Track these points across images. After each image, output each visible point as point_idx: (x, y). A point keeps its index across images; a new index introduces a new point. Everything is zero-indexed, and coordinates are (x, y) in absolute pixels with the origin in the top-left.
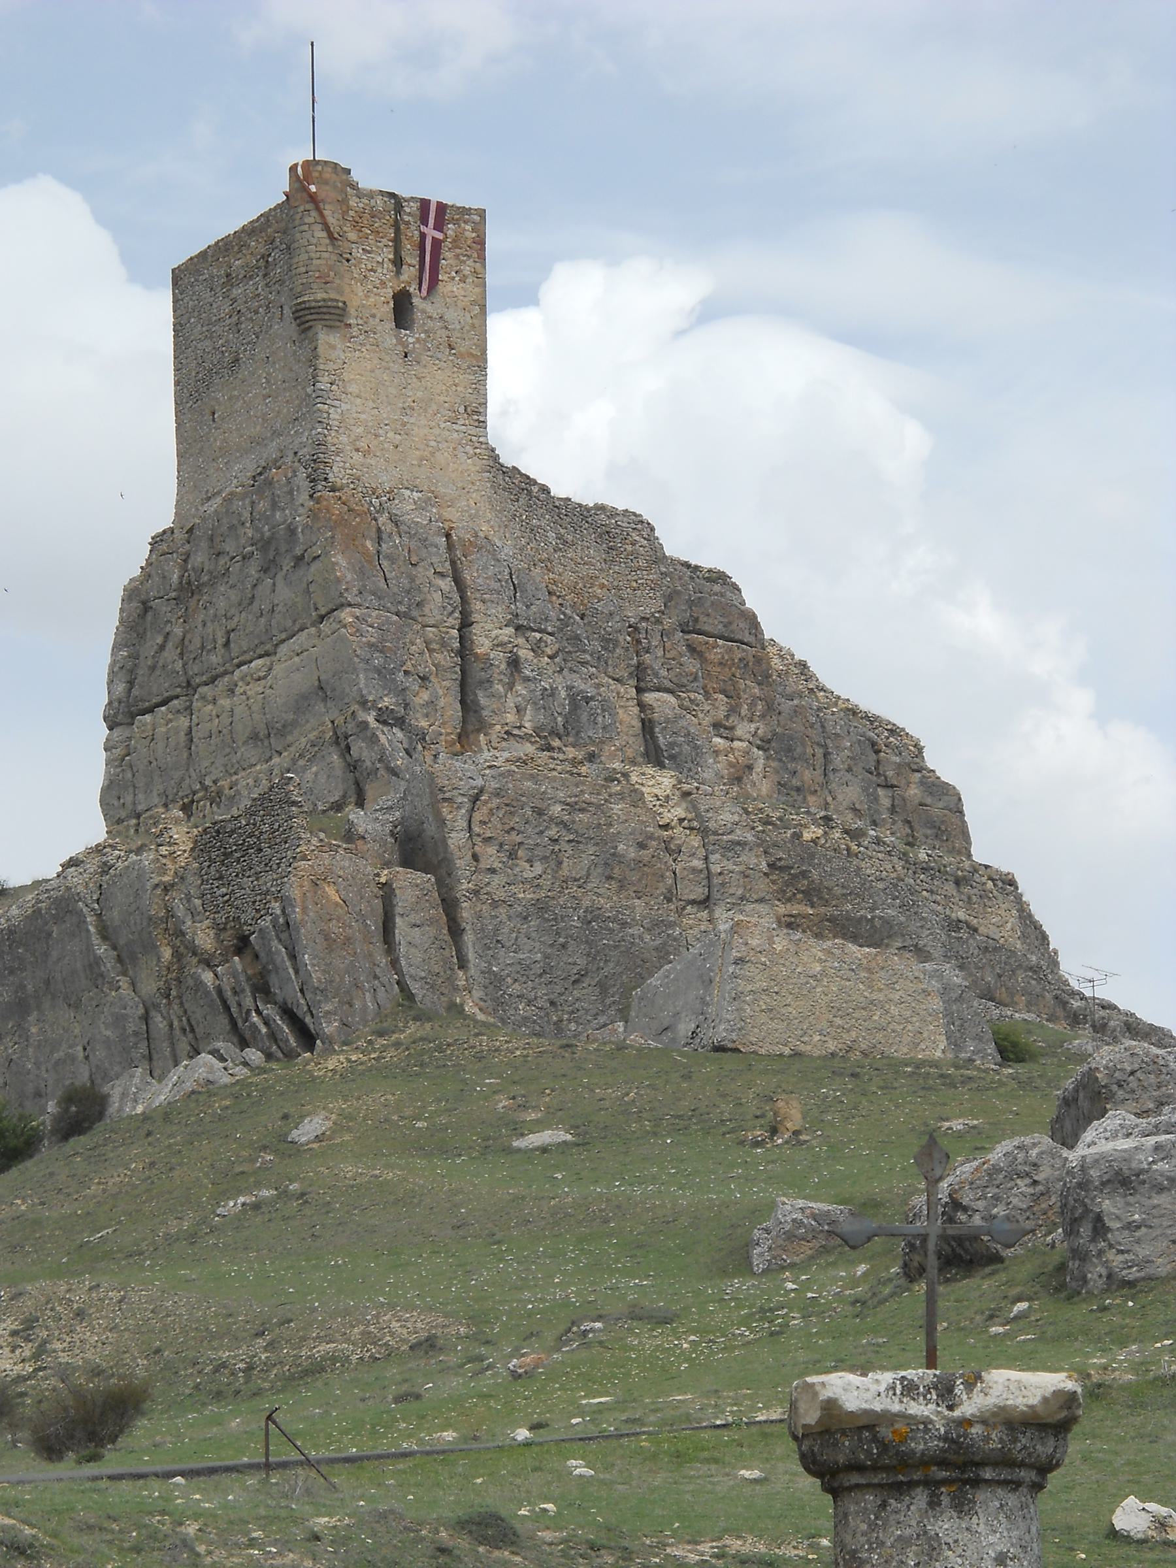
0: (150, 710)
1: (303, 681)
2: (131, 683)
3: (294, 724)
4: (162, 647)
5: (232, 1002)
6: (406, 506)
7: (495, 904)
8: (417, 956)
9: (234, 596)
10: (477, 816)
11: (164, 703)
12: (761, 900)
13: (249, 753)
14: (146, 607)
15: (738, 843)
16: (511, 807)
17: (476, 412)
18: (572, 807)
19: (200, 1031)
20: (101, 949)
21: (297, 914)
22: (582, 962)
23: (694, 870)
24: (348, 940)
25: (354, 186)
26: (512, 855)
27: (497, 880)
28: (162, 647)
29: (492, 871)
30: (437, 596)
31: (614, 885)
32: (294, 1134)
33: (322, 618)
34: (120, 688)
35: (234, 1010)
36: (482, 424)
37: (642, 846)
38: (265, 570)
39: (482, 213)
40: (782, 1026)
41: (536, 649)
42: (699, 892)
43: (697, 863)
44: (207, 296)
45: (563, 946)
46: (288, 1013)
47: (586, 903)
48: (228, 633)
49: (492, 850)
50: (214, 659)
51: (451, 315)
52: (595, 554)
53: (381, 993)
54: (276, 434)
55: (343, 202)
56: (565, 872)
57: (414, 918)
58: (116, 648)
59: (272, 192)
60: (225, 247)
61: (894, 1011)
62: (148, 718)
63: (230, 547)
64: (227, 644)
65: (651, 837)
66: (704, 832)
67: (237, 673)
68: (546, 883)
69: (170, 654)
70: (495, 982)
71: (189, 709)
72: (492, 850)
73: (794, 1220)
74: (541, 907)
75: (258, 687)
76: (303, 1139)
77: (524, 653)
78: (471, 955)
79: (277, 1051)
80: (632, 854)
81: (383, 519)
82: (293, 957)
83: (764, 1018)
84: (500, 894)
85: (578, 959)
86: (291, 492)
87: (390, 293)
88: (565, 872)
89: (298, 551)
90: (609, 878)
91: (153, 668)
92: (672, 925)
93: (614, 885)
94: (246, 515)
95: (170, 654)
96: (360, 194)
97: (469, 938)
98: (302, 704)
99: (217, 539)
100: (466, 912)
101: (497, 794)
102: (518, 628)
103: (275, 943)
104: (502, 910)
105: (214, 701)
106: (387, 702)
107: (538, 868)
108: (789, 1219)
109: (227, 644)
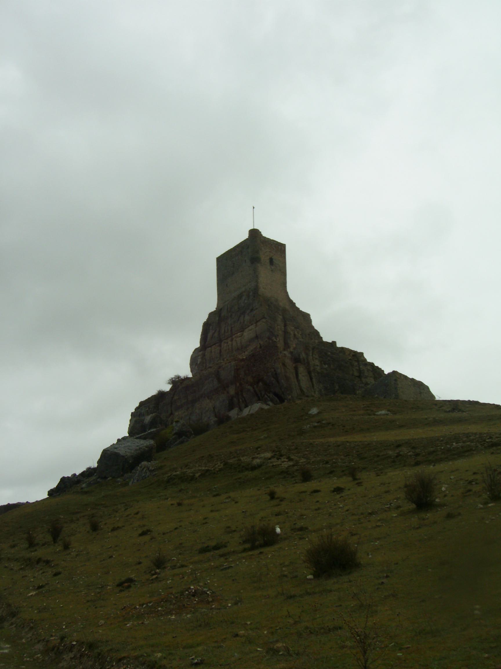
0: (211, 347)
11: (215, 344)
29: (318, 365)
43: (357, 368)
48: (232, 328)
59: (246, 236)
62: (210, 348)
67: (234, 336)
71: (220, 346)
75: (240, 338)
77: (296, 333)
78: (315, 384)
87: (268, 258)
97: (314, 380)
105: (227, 343)
109: (231, 330)
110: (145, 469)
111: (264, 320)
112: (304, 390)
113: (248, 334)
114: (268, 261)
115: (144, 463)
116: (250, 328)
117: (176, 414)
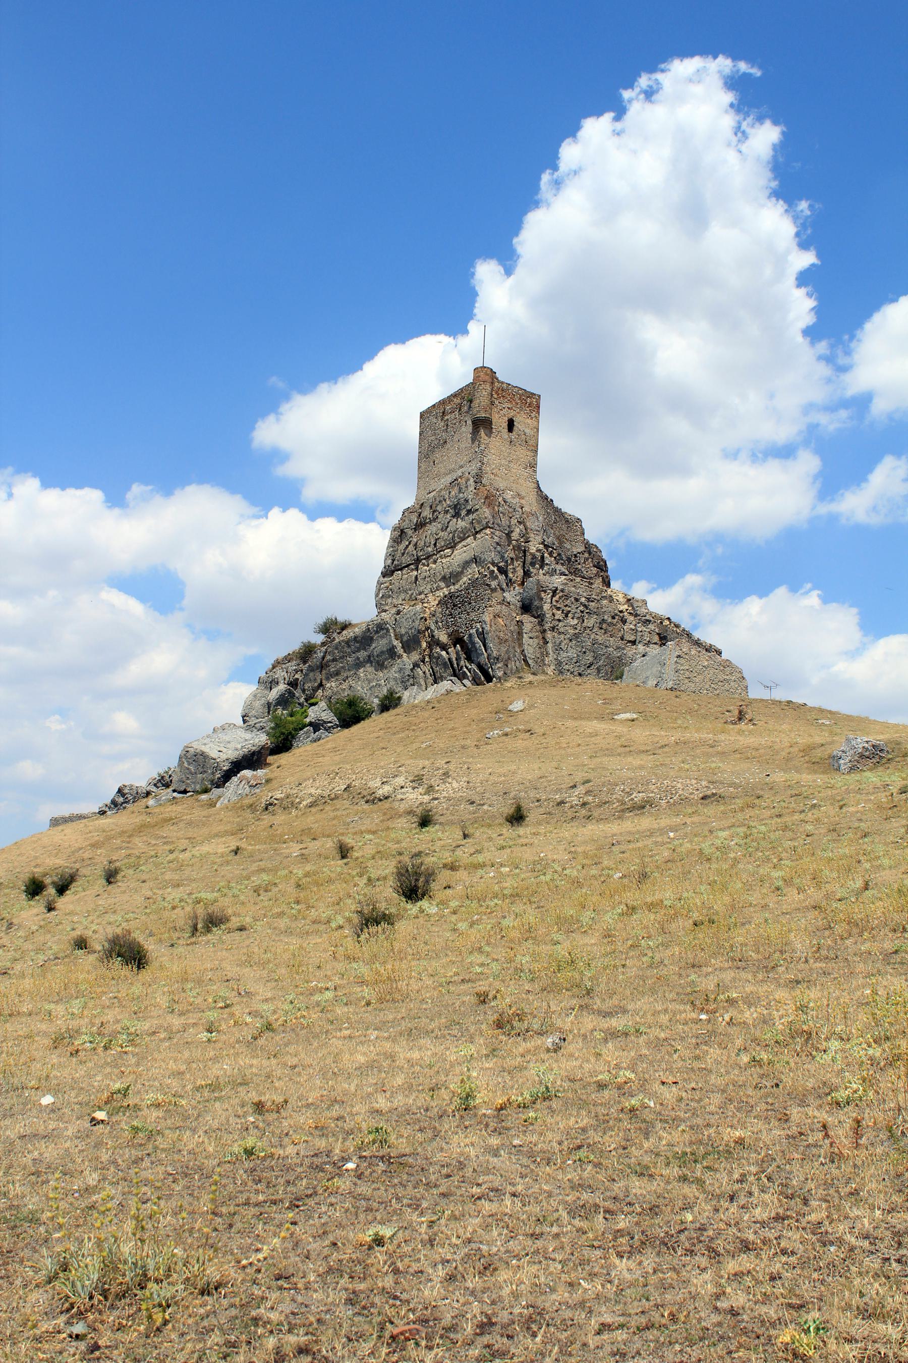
0: (401, 569)
1: (467, 556)
2: (393, 560)
3: (462, 572)
4: (407, 546)
5: (455, 662)
6: (508, 495)
7: (560, 633)
8: (531, 650)
9: (440, 526)
10: (554, 599)
11: (407, 566)
12: (655, 643)
13: (442, 584)
14: (402, 531)
15: (647, 620)
16: (567, 597)
17: (533, 466)
18: (589, 600)
19: (438, 675)
20: (396, 643)
21: (487, 628)
22: (591, 659)
23: (631, 629)
24: (506, 641)
25: (497, 379)
26: (567, 616)
27: (561, 624)
28: (407, 546)
30: (518, 530)
31: (603, 631)
32: (511, 707)
33: (477, 533)
34: (389, 562)
35: (455, 665)
36: (535, 471)
37: (613, 618)
38: (453, 517)
39: (539, 396)
40: (693, 685)
41: (551, 554)
42: (632, 638)
43: (632, 626)
44: (435, 420)
45: (585, 652)
46: (480, 667)
47: (592, 637)
49: (560, 612)
50: (430, 549)
51: (527, 431)
52: (564, 527)
53: (518, 663)
54: (461, 467)
55: (492, 383)
56: (585, 624)
57: (530, 635)
58: (388, 547)
60: (443, 402)
61: (732, 684)
63: (439, 508)
64: (435, 545)
65: (616, 615)
66: (636, 615)
68: (579, 628)
69: (411, 547)
70: (559, 663)
72: (560, 612)
73: (864, 747)
74: (576, 636)
76: (515, 710)
79: (476, 682)
80: (610, 620)
81: (500, 499)
82: (485, 646)
83: (687, 681)
84: (562, 630)
85: (589, 658)
86: (467, 487)
88: (585, 624)
89: (469, 508)
90: (601, 628)
91: (403, 554)
92: (624, 649)
93: (603, 631)
94: (447, 496)
95: (411, 547)
96: (499, 382)
98: (466, 564)
99: (434, 506)
100: (549, 635)
101: (562, 591)
102: (545, 545)
103: (477, 640)
104: (562, 636)
105: (428, 566)
106: (502, 564)
107: (576, 621)
108: (861, 746)
109: (435, 545)
110: (243, 783)
111: (488, 531)
112: (530, 662)
113: (460, 554)
114: (505, 425)
115: (247, 773)
116: (464, 543)
117: (328, 685)
